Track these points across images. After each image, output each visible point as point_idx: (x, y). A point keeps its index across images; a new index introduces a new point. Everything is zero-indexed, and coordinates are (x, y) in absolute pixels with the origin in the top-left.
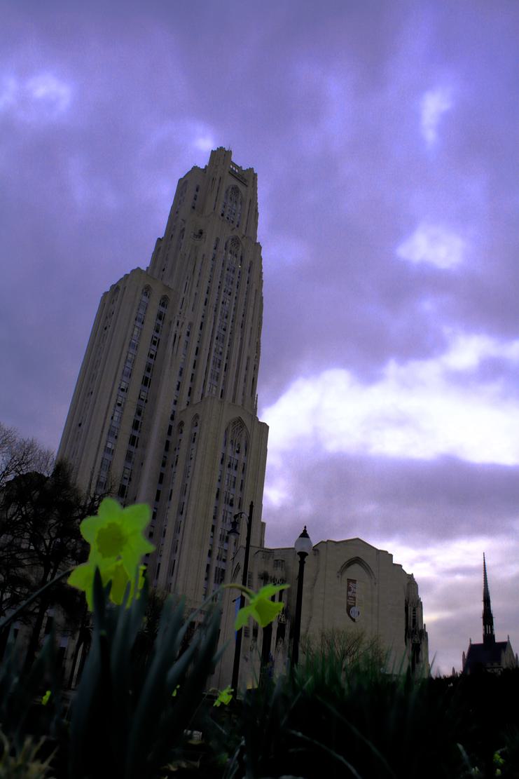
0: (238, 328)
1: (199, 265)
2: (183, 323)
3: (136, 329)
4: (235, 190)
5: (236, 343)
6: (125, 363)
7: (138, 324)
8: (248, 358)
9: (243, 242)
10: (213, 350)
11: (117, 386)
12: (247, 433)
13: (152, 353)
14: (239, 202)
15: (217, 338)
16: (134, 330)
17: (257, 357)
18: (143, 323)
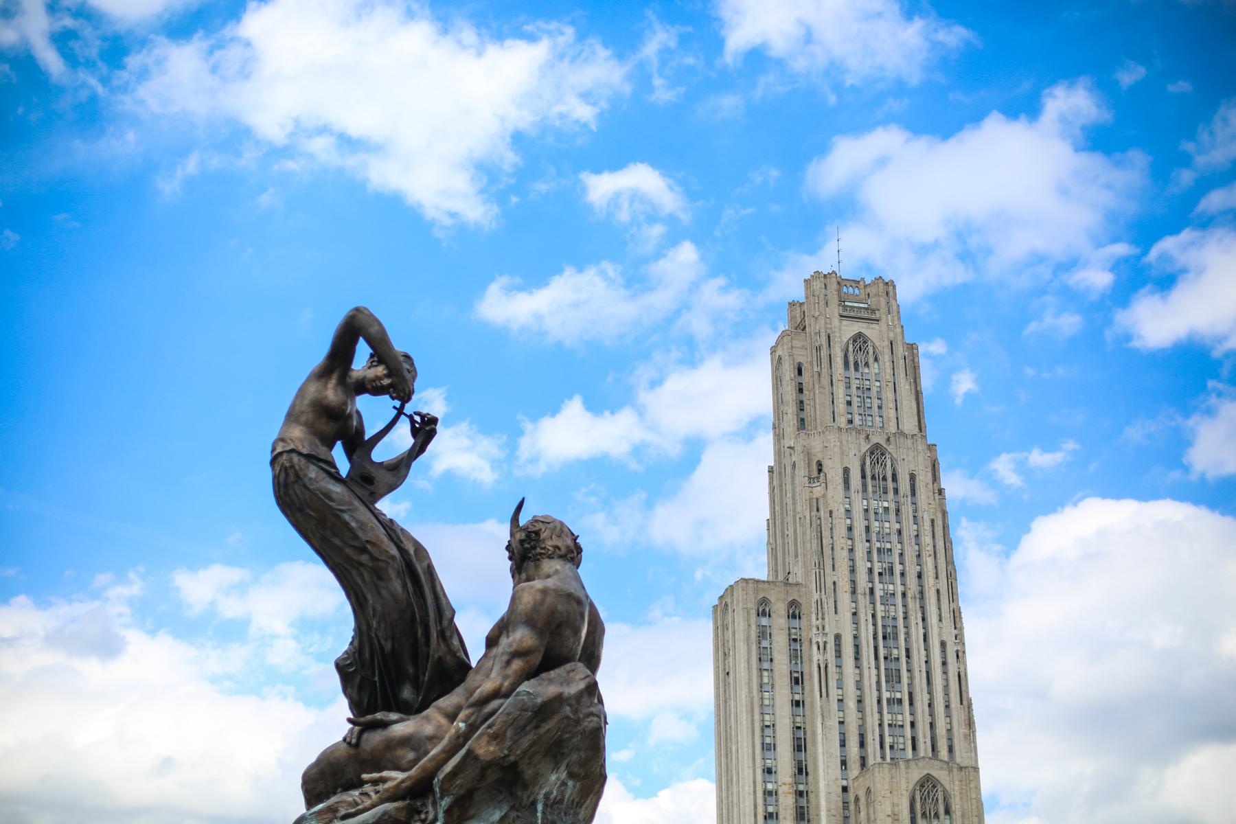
0: (913, 606)
1: (826, 534)
2: (825, 643)
3: (765, 674)
4: (859, 339)
5: (917, 633)
6: (763, 731)
7: (766, 665)
8: (943, 644)
9: (891, 448)
10: (882, 660)
11: (759, 772)
12: (945, 791)
13: (797, 697)
14: (871, 360)
15: (884, 638)
16: (761, 676)
17: (959, 637)
18: (771, 660)
